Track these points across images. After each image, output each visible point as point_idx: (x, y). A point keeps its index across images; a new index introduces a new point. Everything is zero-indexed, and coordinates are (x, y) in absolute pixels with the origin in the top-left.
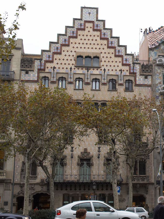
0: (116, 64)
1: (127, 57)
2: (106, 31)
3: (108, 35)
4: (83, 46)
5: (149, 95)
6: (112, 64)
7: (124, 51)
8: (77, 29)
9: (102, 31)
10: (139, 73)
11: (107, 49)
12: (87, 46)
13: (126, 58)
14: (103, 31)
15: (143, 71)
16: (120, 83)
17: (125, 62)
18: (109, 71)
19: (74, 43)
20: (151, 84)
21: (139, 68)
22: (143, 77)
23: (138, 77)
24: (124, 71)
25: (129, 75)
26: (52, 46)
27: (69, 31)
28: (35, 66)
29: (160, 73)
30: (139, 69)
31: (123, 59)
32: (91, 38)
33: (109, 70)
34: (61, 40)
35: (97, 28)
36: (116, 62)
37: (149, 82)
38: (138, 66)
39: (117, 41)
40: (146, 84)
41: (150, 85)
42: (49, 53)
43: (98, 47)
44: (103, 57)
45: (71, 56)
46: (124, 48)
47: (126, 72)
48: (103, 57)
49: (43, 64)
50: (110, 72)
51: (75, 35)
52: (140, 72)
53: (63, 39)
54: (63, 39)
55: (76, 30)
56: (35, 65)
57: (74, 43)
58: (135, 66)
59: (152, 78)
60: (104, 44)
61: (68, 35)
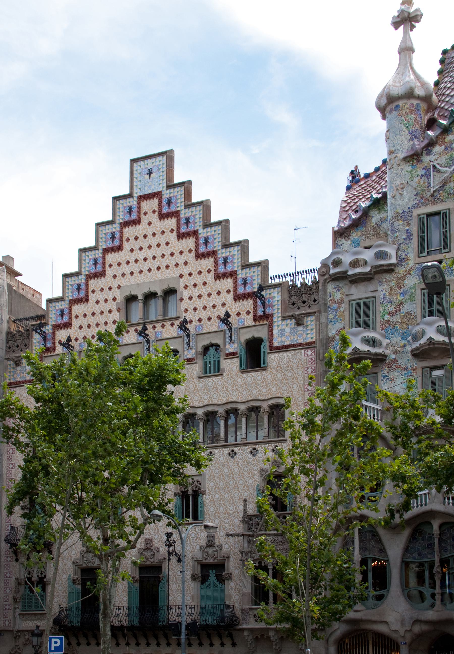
0: (218, 301)
1: (246, 273)
2: (192, 212)
3: (197, 220)
4: (136, 268)
5: (310, 372)
6: (209, 302)
7: (238, 258)
8: (121, 224)
9: (182, 215)
10: (280, 315)
11: (195, 262)
12: (154, 264)
13: (244, 276)
14: (185, 213)
15: (293, 304)
16: (232, 351)
17: (241, 289)
18: (202, 323)
19: (115, 266)
20: (314, 340)
21: (280, 298)
22: (291, 324)
23: (278, 326)
24: (238, 314)
25: (253, 324)
26: (67, 284)
27: (104, 236)
28: (34, 345)
29: (340, 303)
30: (280, 302)
31: (235, 282)
32: (153, 241)
33: (200, 320)
34: (87, 265)
35: (130, 216)
36: (219, 293)
37: (310, 336)
38: (278, 293)
39: (220, 232)
40: (300, 341)
41: (313, 343)
42: (61, 305)
43: (172, 261)
44: (186, 287)
45: (110, 301)
46: (239, 248)
47: (246, 316)
48: (186, 287)
49: (49, 337)
50: (204, 326)
51: (117, 243)
52: (282, 312)
53: (90, 259)
54: (90, 259)
55: (118, 229)
56: (34, 341)
57: (115, 266)
58: (270, 294)
59: (317, 320)
60: (187, 250)
61: (102, 246)
